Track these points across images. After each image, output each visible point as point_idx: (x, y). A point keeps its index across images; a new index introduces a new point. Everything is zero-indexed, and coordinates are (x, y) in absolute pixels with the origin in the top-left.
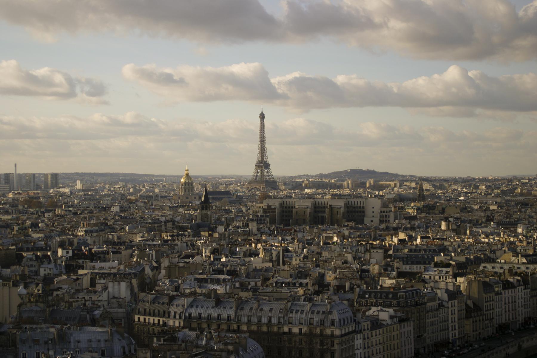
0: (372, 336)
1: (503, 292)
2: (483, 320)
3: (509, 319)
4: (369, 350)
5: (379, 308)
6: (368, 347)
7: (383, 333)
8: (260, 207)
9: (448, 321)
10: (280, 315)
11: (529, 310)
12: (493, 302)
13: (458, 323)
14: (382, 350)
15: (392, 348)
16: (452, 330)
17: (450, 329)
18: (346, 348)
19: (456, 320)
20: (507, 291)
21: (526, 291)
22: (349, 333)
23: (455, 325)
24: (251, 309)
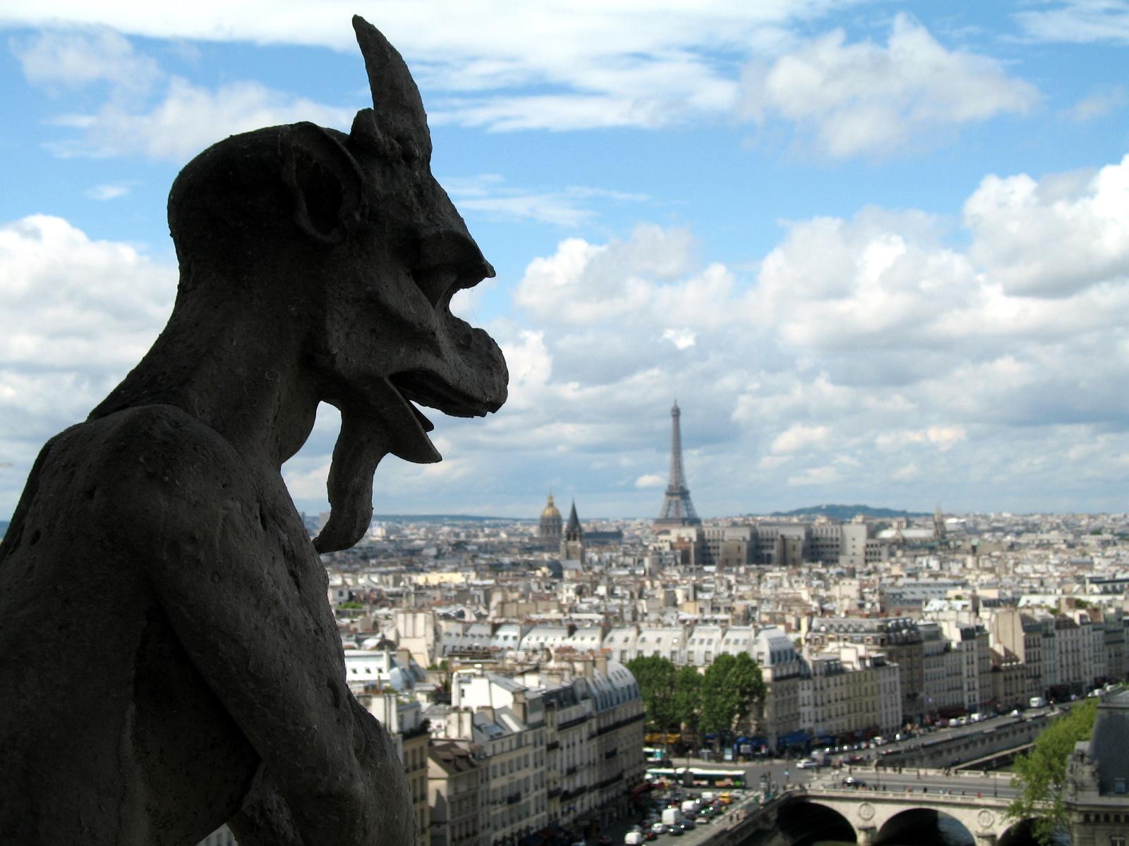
0: (829, 686)
1: (1056, 633)
2: (1022, 676)
3: (1068, 679)
4: (823, 708)
5: (841, 644)
6: (823, 704)
7: (848, 682)
8: (666, 541)
9: (961, 674)
10: (674, 648)
11: (1102, 665)
12: (1040, 649)
13: (980, 679)
14: (845, 710)
15: (864, 708)
16: (969, 690)
17: (966, 687)
18: (783, 701)
19: (976, 673)
20: (1063, 632)
21: (1096, 633)
22: (788, 677)
23: (973, 683)
24: (626, 640)
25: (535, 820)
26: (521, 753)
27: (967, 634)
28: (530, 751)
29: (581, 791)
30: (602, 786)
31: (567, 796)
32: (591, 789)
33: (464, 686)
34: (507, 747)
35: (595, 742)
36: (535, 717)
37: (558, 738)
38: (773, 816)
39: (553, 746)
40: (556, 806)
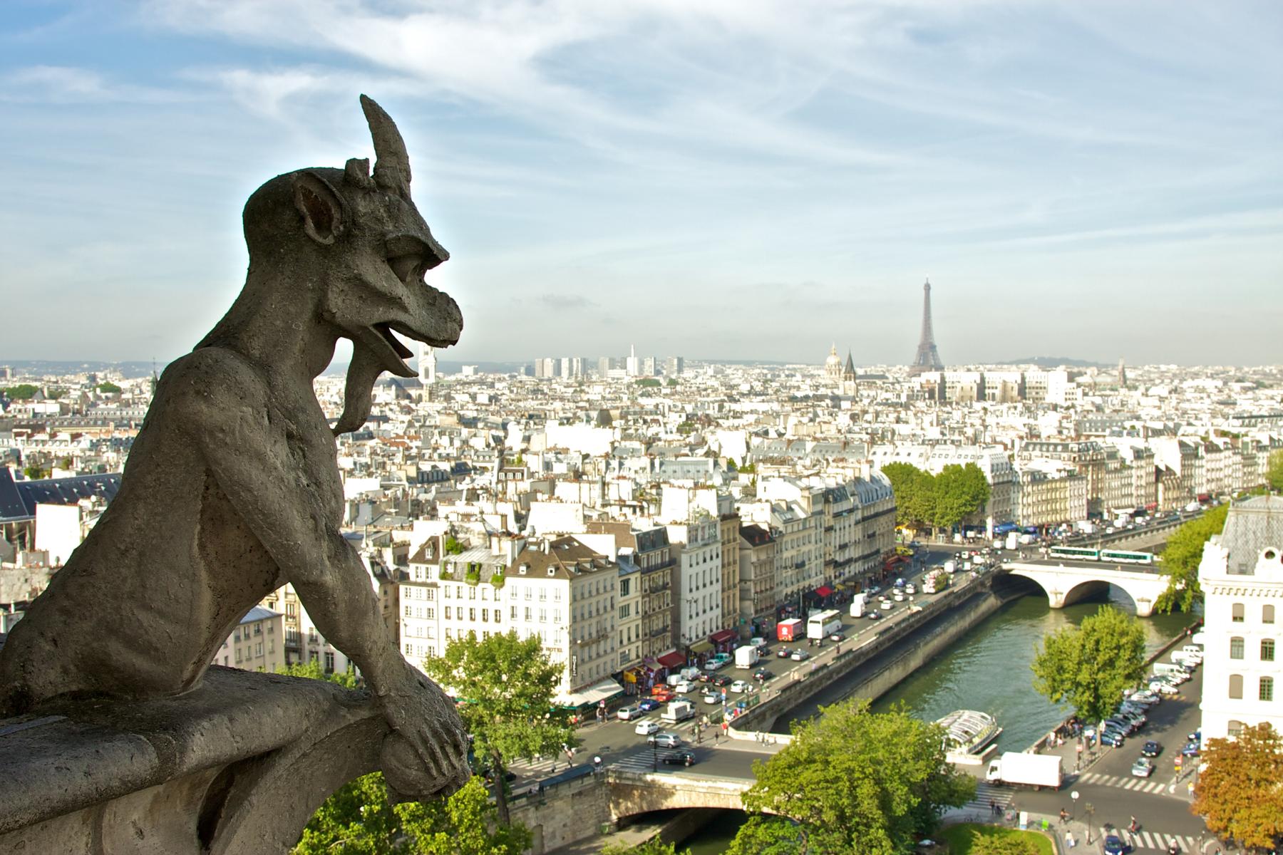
25: (816, 581)
26: (806, 533)
27: (1138, 454)
28: (813, 532)
29: (849, 562)
30: (865, 558)
31: (837, 564)
32: (856, 560)
33: (765, 483)
34: (795, 529)
35: (860, 527)
36: (819, 507)
37: (832, 523)
38: (988, 584)
39: (829, 529)
40: (831, 572)
